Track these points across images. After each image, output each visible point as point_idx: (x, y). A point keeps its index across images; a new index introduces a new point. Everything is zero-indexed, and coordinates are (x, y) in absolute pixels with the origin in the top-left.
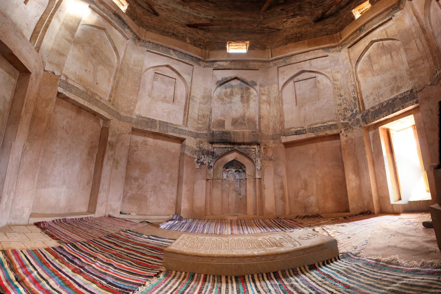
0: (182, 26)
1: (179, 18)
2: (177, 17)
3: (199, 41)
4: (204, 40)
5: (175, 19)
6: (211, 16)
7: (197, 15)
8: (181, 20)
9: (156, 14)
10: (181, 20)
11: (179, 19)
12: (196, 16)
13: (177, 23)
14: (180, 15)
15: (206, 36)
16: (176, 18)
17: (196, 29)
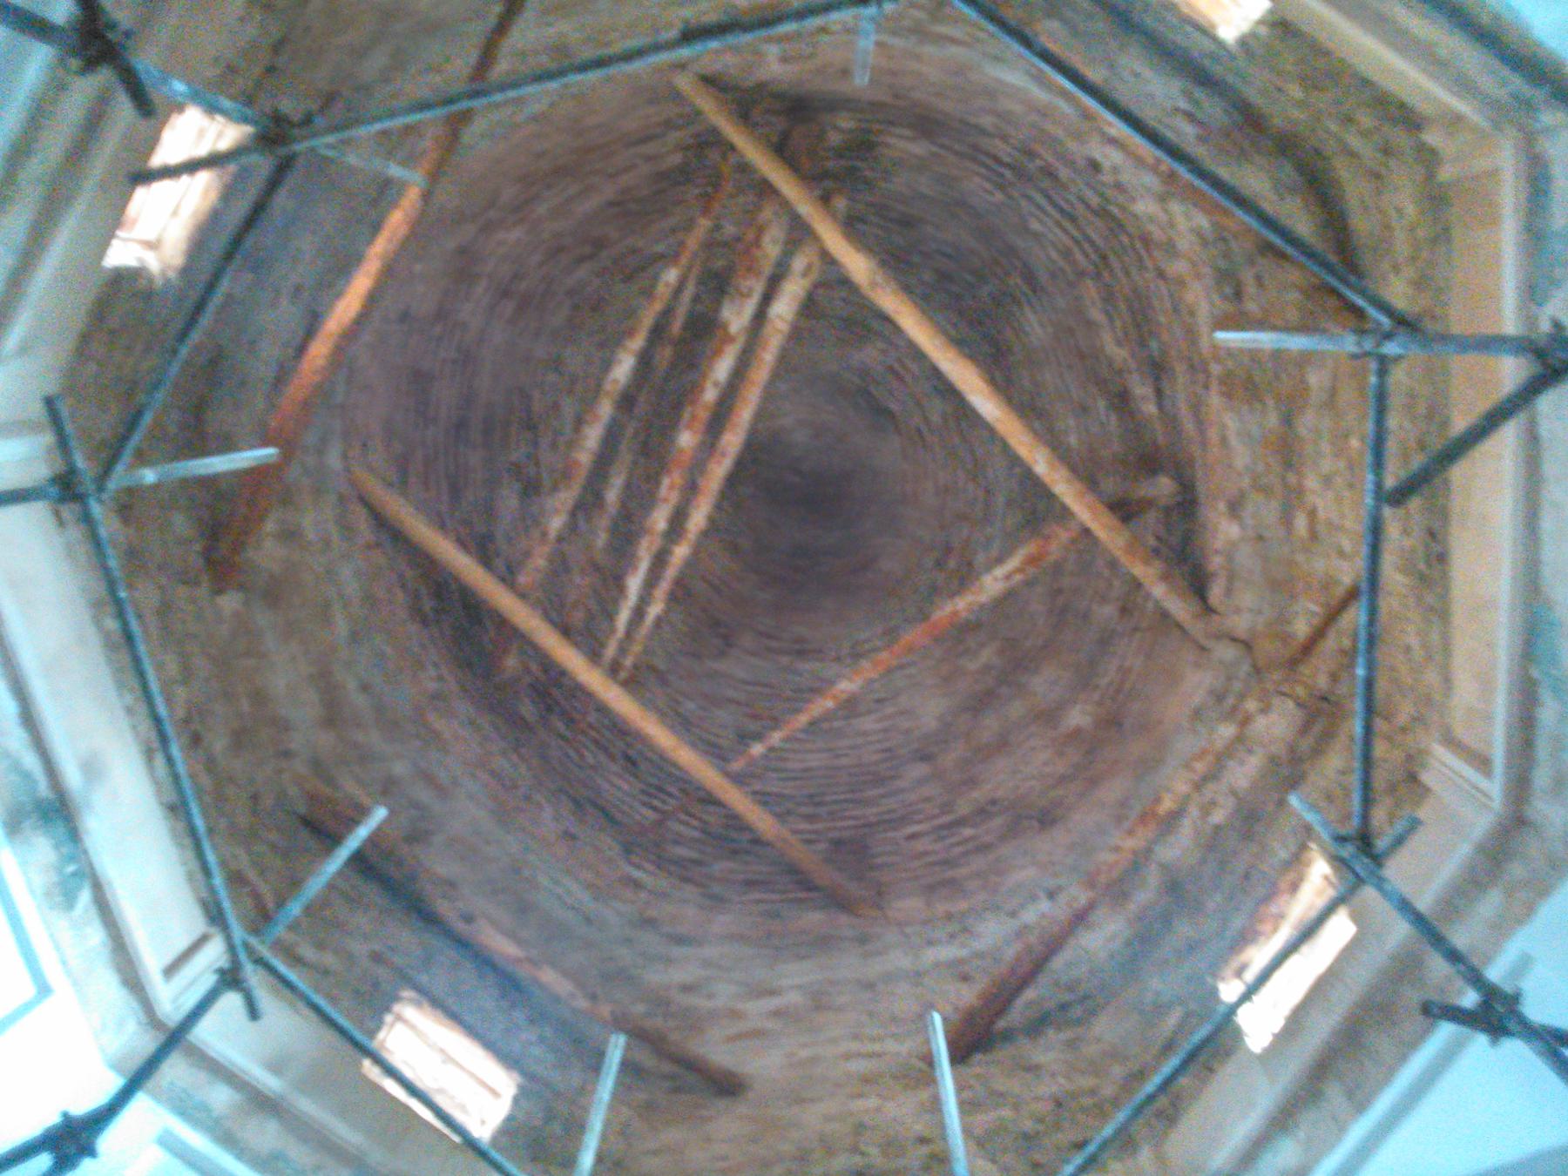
0: (906, 1087)
1: (873, 1040)
2: (856, 1037)
3: (1057, 1126)
4: (1093, 1092)
5: (847, 1057)
6: (1034, 898)
7: (963, 953)
8: (891, 1046)
9: (728, 1086)
10: (891, 1046)
11: (877, 1047)
12: (961, 961)
13: (866, 1080)
14: (871, 1014)
15: (1091, 1050)
16: (854, 1046)
17: (1003, 1053)
